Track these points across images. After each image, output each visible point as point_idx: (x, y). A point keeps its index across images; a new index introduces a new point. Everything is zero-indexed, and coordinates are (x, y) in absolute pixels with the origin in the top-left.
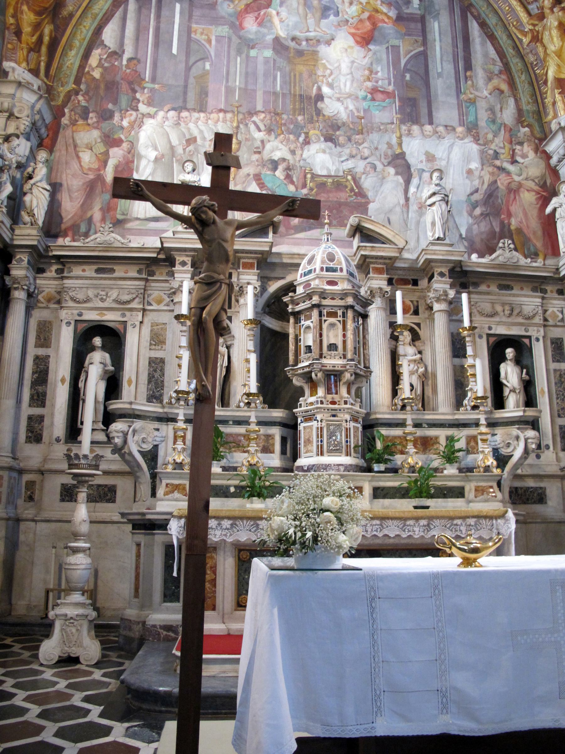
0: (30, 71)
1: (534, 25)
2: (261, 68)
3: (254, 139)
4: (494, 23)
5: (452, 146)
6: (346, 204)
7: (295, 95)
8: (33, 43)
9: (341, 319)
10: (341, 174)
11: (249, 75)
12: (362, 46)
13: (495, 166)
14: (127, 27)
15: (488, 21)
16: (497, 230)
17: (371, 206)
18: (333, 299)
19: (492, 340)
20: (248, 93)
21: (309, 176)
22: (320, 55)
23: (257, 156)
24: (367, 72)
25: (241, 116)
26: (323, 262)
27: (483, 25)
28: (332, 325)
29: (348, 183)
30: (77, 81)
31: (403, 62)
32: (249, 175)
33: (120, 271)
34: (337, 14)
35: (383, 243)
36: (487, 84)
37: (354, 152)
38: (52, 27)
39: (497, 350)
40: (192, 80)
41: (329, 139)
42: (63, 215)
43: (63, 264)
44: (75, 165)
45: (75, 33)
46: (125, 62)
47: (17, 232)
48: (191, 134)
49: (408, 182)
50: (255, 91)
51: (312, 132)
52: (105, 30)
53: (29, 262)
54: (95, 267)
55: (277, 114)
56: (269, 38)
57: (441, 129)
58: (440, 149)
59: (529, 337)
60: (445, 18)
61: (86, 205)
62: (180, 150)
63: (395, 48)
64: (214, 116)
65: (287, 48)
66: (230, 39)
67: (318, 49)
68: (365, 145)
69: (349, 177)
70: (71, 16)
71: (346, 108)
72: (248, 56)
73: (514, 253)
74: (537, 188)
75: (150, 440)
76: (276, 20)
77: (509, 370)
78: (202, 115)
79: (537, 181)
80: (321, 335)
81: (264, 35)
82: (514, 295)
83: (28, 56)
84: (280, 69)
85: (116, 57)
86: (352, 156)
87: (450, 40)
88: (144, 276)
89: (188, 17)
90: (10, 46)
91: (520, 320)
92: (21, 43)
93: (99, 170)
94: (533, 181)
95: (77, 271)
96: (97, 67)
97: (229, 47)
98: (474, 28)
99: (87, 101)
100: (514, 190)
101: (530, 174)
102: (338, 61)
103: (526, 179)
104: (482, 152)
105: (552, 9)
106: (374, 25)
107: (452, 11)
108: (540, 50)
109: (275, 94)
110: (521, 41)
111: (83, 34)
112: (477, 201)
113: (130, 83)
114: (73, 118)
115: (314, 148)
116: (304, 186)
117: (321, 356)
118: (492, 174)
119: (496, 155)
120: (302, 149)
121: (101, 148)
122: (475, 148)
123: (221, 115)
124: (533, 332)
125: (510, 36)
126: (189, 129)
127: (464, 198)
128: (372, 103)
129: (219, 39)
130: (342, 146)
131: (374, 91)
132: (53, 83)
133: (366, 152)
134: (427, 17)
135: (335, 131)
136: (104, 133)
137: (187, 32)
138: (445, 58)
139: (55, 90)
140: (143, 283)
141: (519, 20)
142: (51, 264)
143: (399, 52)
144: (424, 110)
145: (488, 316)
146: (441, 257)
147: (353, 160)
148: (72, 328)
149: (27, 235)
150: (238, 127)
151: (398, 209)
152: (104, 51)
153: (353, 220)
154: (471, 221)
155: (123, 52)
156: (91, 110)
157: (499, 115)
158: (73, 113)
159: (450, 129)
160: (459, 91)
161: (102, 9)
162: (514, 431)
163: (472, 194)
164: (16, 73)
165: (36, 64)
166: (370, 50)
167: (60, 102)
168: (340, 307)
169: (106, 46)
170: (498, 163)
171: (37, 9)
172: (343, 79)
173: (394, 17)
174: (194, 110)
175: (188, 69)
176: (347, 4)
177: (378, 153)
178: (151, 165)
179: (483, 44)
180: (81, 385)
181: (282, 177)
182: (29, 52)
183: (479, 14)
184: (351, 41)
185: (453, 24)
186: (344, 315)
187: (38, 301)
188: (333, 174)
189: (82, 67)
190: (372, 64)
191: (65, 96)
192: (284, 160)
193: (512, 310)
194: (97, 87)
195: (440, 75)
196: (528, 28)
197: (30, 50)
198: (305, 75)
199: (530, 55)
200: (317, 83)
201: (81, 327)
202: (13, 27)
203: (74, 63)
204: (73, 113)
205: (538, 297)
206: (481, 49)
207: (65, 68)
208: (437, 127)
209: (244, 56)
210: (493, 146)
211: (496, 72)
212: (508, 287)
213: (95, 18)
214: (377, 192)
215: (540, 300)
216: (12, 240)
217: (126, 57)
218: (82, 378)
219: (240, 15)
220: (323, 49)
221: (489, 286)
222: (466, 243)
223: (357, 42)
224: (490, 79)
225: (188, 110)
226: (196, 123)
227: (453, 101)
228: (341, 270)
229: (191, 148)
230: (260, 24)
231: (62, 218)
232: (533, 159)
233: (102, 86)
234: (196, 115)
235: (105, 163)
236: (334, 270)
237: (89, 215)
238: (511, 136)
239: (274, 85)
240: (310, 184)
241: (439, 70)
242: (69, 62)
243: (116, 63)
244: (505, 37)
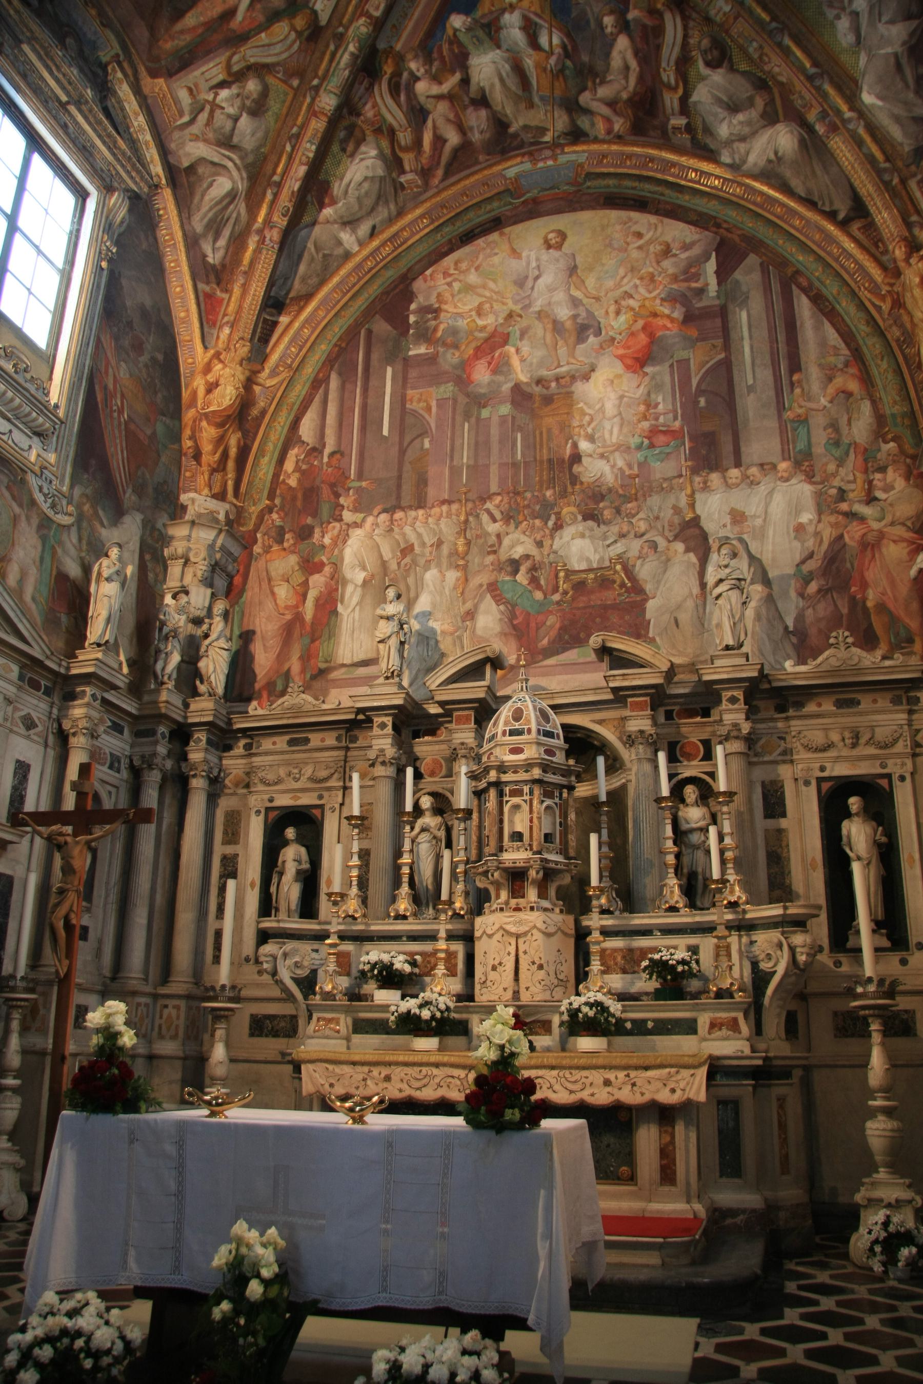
0: (214, 496)
1: (892, 285)
2: (495, 432)
3: (488, 534)
4: (835, 292)
5: (771, 493)
6: (614, 607)
7: (542, 462)
9: (527, 798)
10: (607, 564)
11: (480, 446)
12: (634, 372)
13: (838, 512)
15: (824, 291)
16: (845, 611)
17: (651, 605)
18: (515, 772)
19: (826, 786)
20: (478, 470)
21: (562, 574)
22: (575, 396)
23: (491, 558)
24: (642, 408)
25: (470, 505)
26: (506, 723)
27: (817, 299)
28: (517, 807)
29: (616, 577)
30: (271, 496)
31: (695, 382)
32: (481, 585)
33: (315, 739)
34: (598, 333)
35: (642, 666)
36: (825, 388)
37: (625, 528)
38: (239, 435)
39: (835, 801)
40: (407, 467)
41: (590, 516)
42: (257, 670)
43: (251, 737)
44: (270, 605)
46: (325, 459)
47: (193, 707)
48: (406, 541)
49: (704, 561)
50: (487, 466)
51: (565, 511)
53: (209, 742)
54: (287, 737)
55: (517, 493)
56: (507, 387)
57: (754, 470)
58: (751, 502)
59: (889, 776)
60: (757, 303)
61: (282, 656)
62: (393, 566)
63: (684, 364)
64: (436, 510)
65: (529, 397)
66: (455, 401)
67: (573, 388)
68: (641, 515)
69: (618, 567)
70: (263, 412)
71: (613, 467)
72: (478, 419)
73: (855, 650)
74: (909, 535)
75: (306, 963)
76: (515, 362)
77: (854, 830)
78: (421, 512)
79: (909, 524)
80: (501, 821)
81: (499, 385)
82: (861, 714)
84: (520, 429)
86: (622, 536)
87: (765, 333)
88: (343, 744)
89: (402, 382)
91: (872, 751)
93: (297, 607)
94: (903, 524)
95: (267, 744)
97: (454, 410)
98: (804, 307)
99: (283, 519)
100: (871, 545)
101: (898, 514)
102: (600, 400)
103: (892, 524)
104: (819, 495)
105: (907, 260)
106: (651, 336)
107: (767, 289)
108: (905, 318)
109: (515, 465)
110: (878, 309)
112: (811, 572)
113: (332, 486)
115: (568, 532)
116: (556, 589)
117: (501, 849)
118: (835, 525)
119: (842, 495)
120: (552, 537)
121: (299, 578)
122: (804, 490)
123: (445, 508)
124: (893, 768)
125: (861, 306)
126: (404, 535)
127: (790, 570)
128: (649, 453)
129: (441, 403)
130: (607, 523)
131: (654, 432)
133: (642, 526)
134: (731, 307)
135: (597, 503)
137: (400, 401)
138: (758, 362)
140: (342, 753)
141: (872, 280)
142: (238, 739)
143: (689, 369)
144: (727, 447)
145: (818, 750)
146: (725, 676)
147: (623, 541)
148: (262, 817)
149: (203, 709)
150: (466, 521)
151: (690, 604)
153: (595, 640)
154: (801, 603)
155: (324, 446)
157: (845, 430)
159: (767, 467)
160: (781, 408)
162: (775, 935)
163: (803, 562)
166: (646, 374)
167: (251, 527)
168: (526, 782)
170: (844, 506)
171: (218, 420)
172: (607, 425)
173: (681, 318)
174: (410, 507)
175: (402, 452)
176: (612, 315)
177: (659, 525)
178: (359, 590)
179: (818, 327)
180: (273, 889)
181: (525, 582)
182: (211, 474)
183: (811, 285)
184: (619, 368)
185: (769, 307)
186: (531, 793)
187: (225, 786)
188: (595, 566)
189: (276, 475)
190: (649, 394)
192: (527, 557)
193: (857, 736)
194: (294, 499)
195: (751, 389)
196: (885, 289)
197: (213, 471)
198: (556, 431)
199: (894, 328)
200: (571, 437)
201: (273, 815)
205: (902, 711)
206: (815, 335)
208: (748, 468)
209: (473, 420)
210: (836, 482)
211: (840, 366)
212: (854, 703)
214: (659, 582)
215: (905, 716)
216: (186, 717)
217: (327, 451)
218: (275, 880)
219: (466, 365)
220: (579, 388)
221: (819, 705)
222: (794, 640)
223: (628, 367)
224: (830, 379)
225: (402, 509)
226: (413, 525)
227: (773, 424)
228: (529, 731)
229: (407, 560)
230: (495, 372)
231: (255, 676)
232: (902, 491)
233: (300, 495)
234: (413, 513)
235: (304, 596)
236: (519, 732)
237: (286, 667)
238: (866, 461)
239: (514, 453)
240: (563, 586)
241: (750, 382)
244: (852, 309)
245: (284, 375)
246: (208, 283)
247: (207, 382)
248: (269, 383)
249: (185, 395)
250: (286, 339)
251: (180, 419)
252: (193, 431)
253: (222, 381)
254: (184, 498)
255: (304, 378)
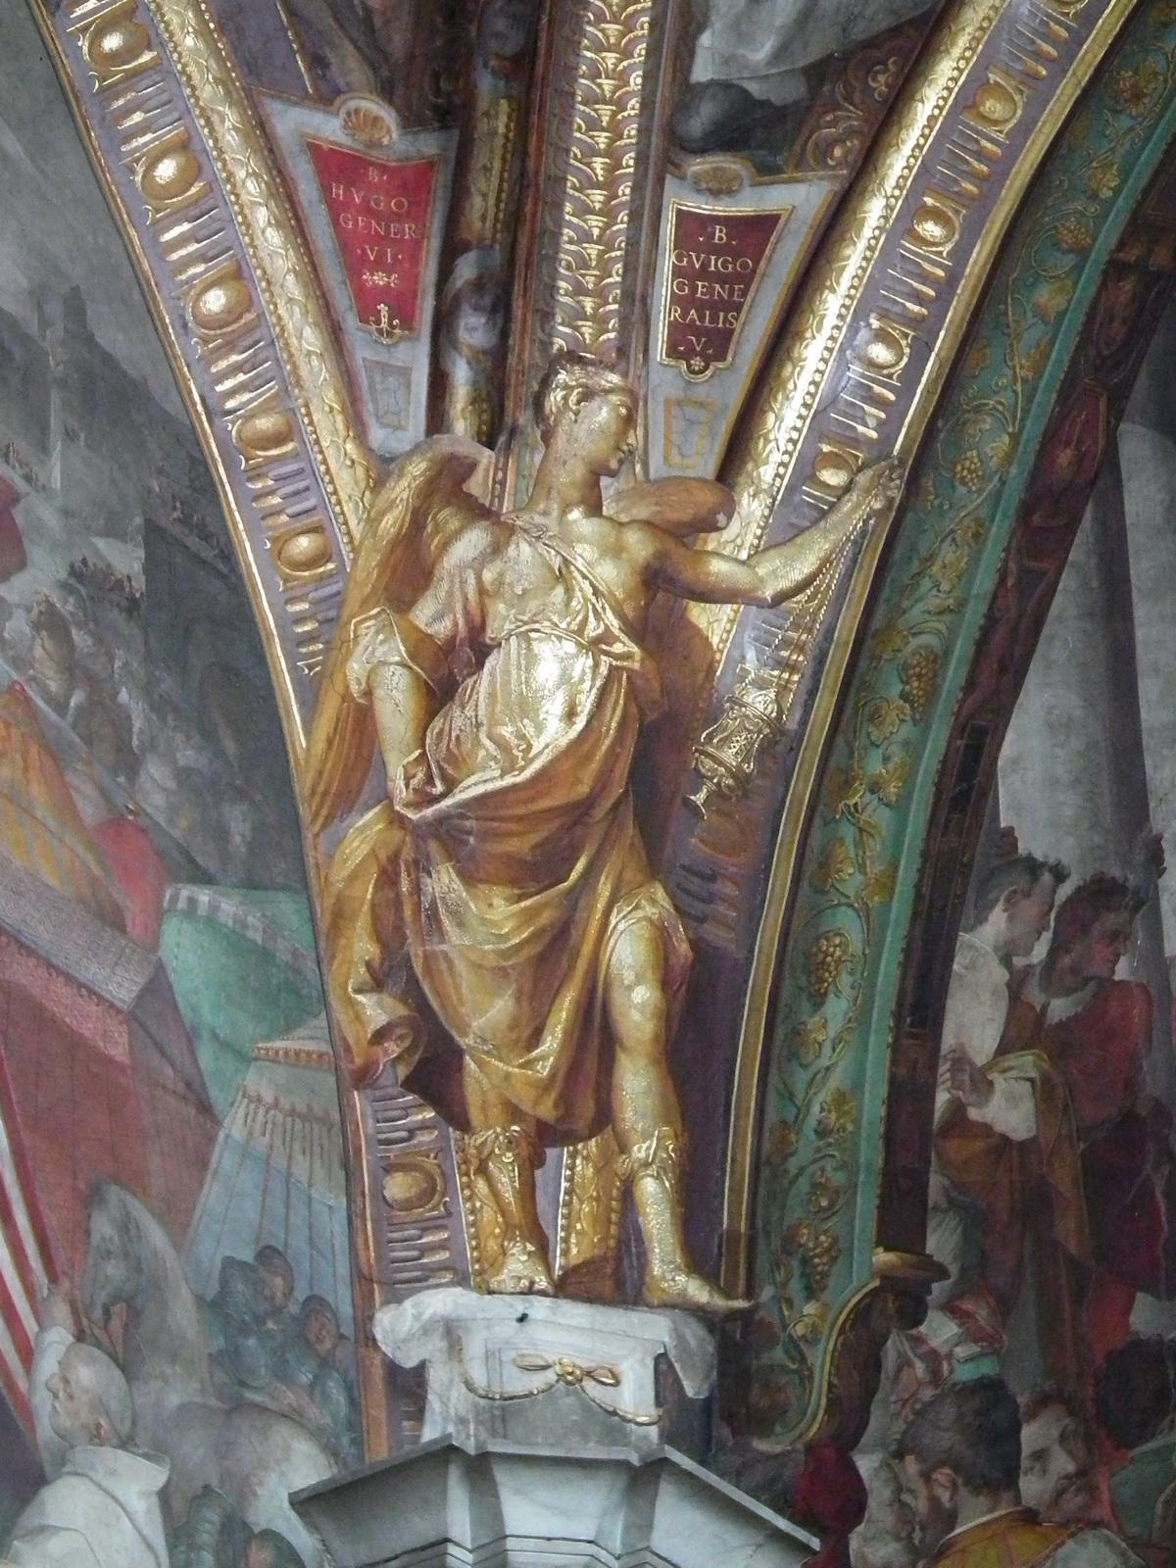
0: (570, 1286)
8: (546, 1086)
14: (1143, 658)
30: (901, 1219)
38: (656, 902)
45: (825, 864)
52: (1007, 750)
83: (528, 1191)
85: (1111, 920)
90: (398, 1187)
92: (464, 1126)
96: (1003, 1050)
99: (988, 1342)
111: (875, 846)
114: (921, 1505)
132: (749, 1293)
136: (1134, 1543)
139: (772, 1341)
152: (1029, 909)
156: (1022, 1400)
158: (912, 1465)
161: (962, 604)
164: (475, 1347)
165: (601, 1220)
169: (1033, 867)
171: (520, 845)
182: (532, 1161)
189: (908, 1093)
191: (844, 1355)
194: (1036, 1205)
202: (393, 1048)
203: (858, 1085)
204: (912, 1465)
207: (806, 1144)
213: (932, 693)
233: (1064, 1178)
242: (824, 1096)
243: (1122, 971)
245: (855, 514)
246: (326, 97)
247: (420, 646)
248: (783, 572)
249: (306, 739)
250: (833, 303)
251: (300, 882)
252: (390, 938)
253: (501, 619)
254: (401, 1326)
255: (971, 499)
